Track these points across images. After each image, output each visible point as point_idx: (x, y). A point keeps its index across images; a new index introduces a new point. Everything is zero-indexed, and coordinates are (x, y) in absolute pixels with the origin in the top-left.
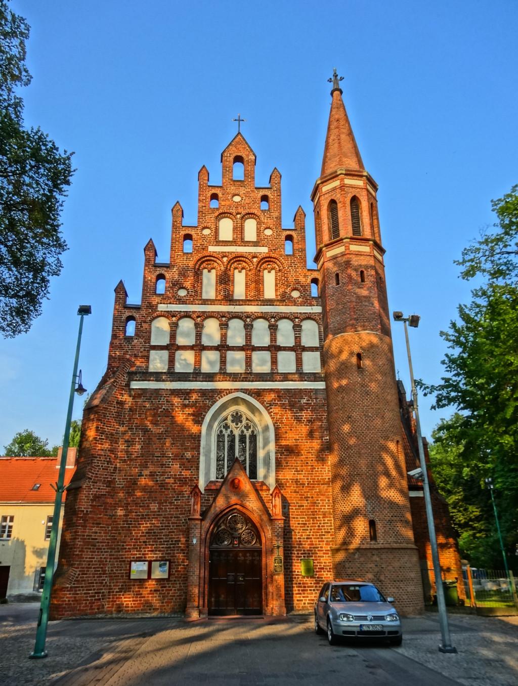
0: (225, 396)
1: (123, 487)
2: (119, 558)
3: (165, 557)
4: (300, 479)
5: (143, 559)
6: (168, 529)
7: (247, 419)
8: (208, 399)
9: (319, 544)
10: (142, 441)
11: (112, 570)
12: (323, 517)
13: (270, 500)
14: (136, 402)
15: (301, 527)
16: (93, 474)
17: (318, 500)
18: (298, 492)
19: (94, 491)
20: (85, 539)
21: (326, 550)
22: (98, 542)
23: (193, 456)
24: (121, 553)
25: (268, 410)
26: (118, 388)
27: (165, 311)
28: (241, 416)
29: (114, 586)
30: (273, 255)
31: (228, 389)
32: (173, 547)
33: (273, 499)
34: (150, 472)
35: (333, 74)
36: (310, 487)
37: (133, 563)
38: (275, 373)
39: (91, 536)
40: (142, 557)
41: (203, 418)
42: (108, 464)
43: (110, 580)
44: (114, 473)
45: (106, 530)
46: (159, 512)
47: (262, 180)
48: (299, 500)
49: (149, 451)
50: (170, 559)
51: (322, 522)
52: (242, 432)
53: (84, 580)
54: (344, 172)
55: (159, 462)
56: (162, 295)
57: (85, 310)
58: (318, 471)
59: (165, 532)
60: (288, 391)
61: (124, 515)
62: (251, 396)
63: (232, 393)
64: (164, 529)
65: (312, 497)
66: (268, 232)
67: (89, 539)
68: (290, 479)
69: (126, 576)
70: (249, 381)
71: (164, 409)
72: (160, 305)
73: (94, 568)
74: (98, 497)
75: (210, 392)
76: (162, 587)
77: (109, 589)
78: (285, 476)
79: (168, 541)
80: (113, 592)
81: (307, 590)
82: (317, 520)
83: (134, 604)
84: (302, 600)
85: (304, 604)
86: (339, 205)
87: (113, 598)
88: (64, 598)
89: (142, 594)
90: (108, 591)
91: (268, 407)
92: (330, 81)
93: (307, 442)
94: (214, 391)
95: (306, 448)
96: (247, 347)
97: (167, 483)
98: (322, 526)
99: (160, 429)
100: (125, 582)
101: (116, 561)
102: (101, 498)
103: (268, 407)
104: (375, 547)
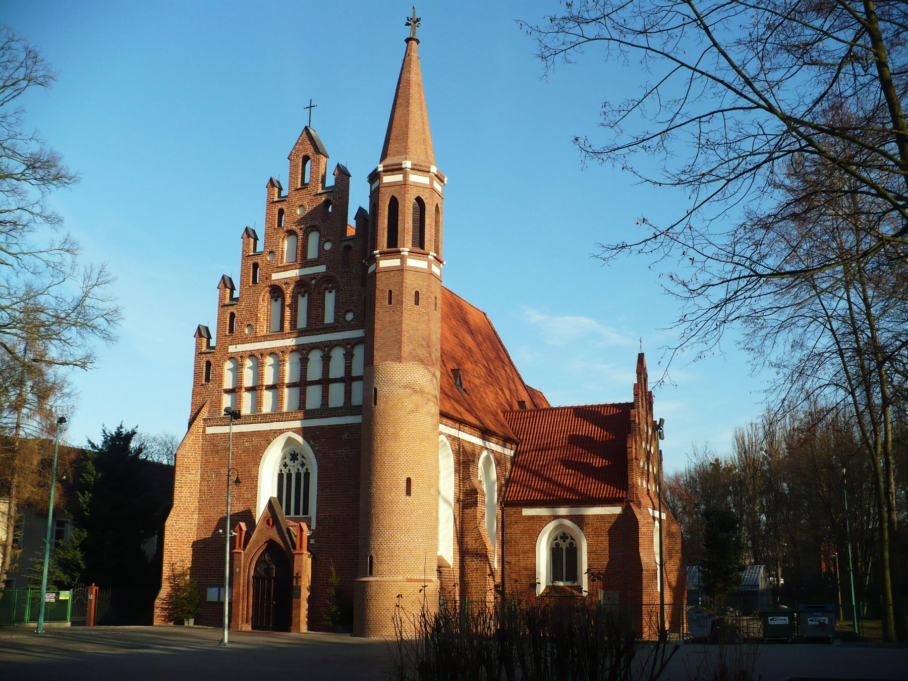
7: (303, 457)
30: (331, 274)
66: (328, 246)
72: (230, 347)
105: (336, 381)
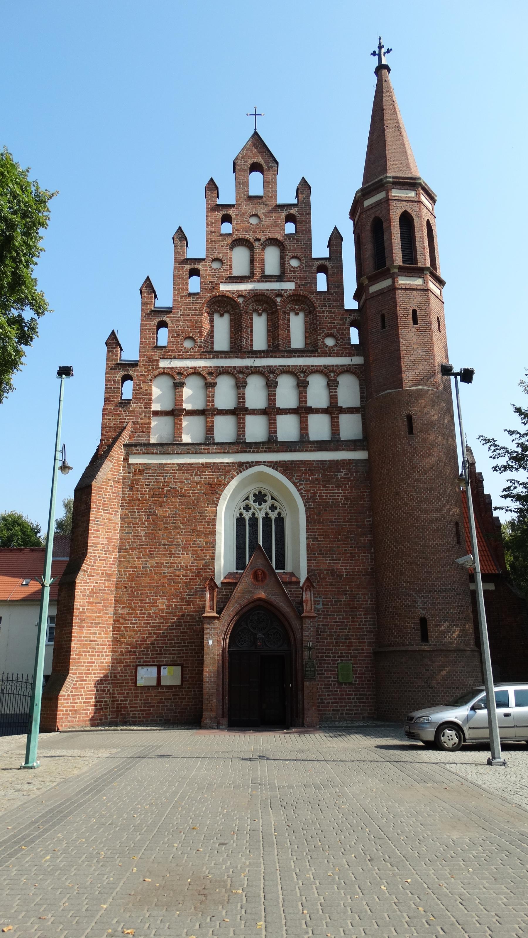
0: (244, 470)
1: (124, 581)
2: (123, 663)
3: (177, 661)
4: (337, 569)
5: (151, 663)
6: (179, 629)
7: (273, 498)
8: (225, 475)
9: (360, 646)
10: (146, 527)
11: (115, 677)
12: (365, 615)
13: (300, 594)
14: (136, 480)
15: (337, 625)
16: (89, 565)
17: (358, 594)
18: (335, 585)
19: (90, 586)
20: (82, 641)
21: (367, 653)
22: (98, 645)
23: (207, 544)
24: (125, 657)
25: (297, 487)
26: (115, 463)
27: (168, 368)
28: (265, 495)
29: (118, 694)
31: (248, 463)
32: (186, 650)
33: (304, 593)
34: (156, 563)
35: (377, 44)
36: (349, 578)
37: (139, 668)
38: (306, 441)
39: (90, 637)
40: (149, 662)
41: (219, 498)
42: (106, 554)
43: (113, 687)
44: (114, 565)
45: (106, 631)
46: (168, 609)
47: (286, 195)
48: (335, 595)
49: (155, 539)
50: (183, 664)
51: (364, 620)
52: (267, 514)
53: (84, 688)
54: (391, 180)
55: (167, 551)
56: (165, 347)
57: (65, 372)
58: (358, 560)
59: (176, 633)
60: (322, 463)
61: (128, 614)
62: (276, 470)
63: (253, 466)
64: (175, 629)
65: (352, 591)
67: (87, 641)
68: (325, 570)
69: (132, 683)
70: (274, 451)
71: (171, 488)
73: (94, 674)
74: (96, 593)
75: (225, 466)
76: (173, 695)
77: (113, 697)
78: (319, 566)
79: (180, 643)
80: (118, 701)
81: (345, 699)
82: (357, 618)
83: (142, 714)
84: (339, 710)
85: (342, 714)
86: (385, 225)
87: (117, 707)
88: (61, 707)
89: (150, 703)
90: (112, 699)
91: (297, 483)
92: (374, 54)
93: (345, 525)
94: (228, 464)
95: (345, 532)
96: (271, 410)
97: (176, 576)
98: (363, 625)
99: (167, 511)
100: (130, 690)
101: (120, 666)
102: (99, 593)
103: (297, 483)
104: (426, 648)
105: (317, 411)
